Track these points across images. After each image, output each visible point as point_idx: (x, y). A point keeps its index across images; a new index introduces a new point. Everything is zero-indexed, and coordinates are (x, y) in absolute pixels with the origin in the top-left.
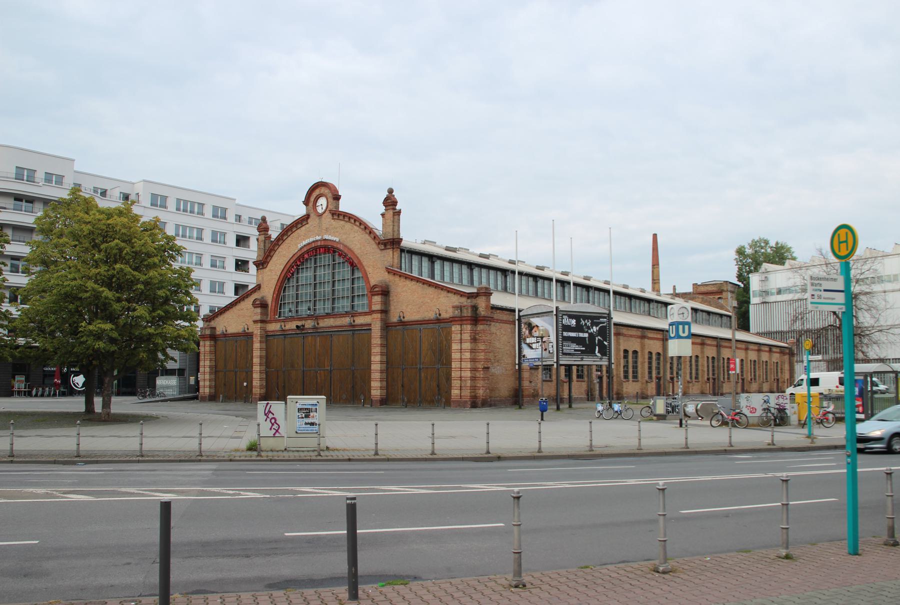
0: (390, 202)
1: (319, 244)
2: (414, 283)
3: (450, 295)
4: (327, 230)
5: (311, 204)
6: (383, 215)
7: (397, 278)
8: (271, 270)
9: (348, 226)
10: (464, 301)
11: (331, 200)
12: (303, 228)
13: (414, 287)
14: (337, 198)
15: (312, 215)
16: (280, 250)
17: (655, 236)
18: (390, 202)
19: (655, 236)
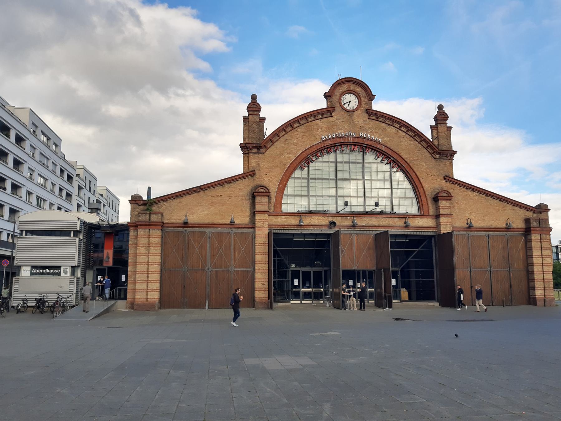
0: (441, 117)
1: (351, 140)
2: (475, 194)
3: (515, 208)
4: (361, 128)
5: (335, 98)
6: (432, 127)
7: (457, 187)
8: (271, 157)
9: (391, 130)
10: (530, 214)
11: (364, 100)
12: (326, 120)
13: (477, 197)
14: (371, 97)
15: (338, 109)
16: (287, 136)
17: (149, 188)
18: (441, 117)
19: (149, 188)
